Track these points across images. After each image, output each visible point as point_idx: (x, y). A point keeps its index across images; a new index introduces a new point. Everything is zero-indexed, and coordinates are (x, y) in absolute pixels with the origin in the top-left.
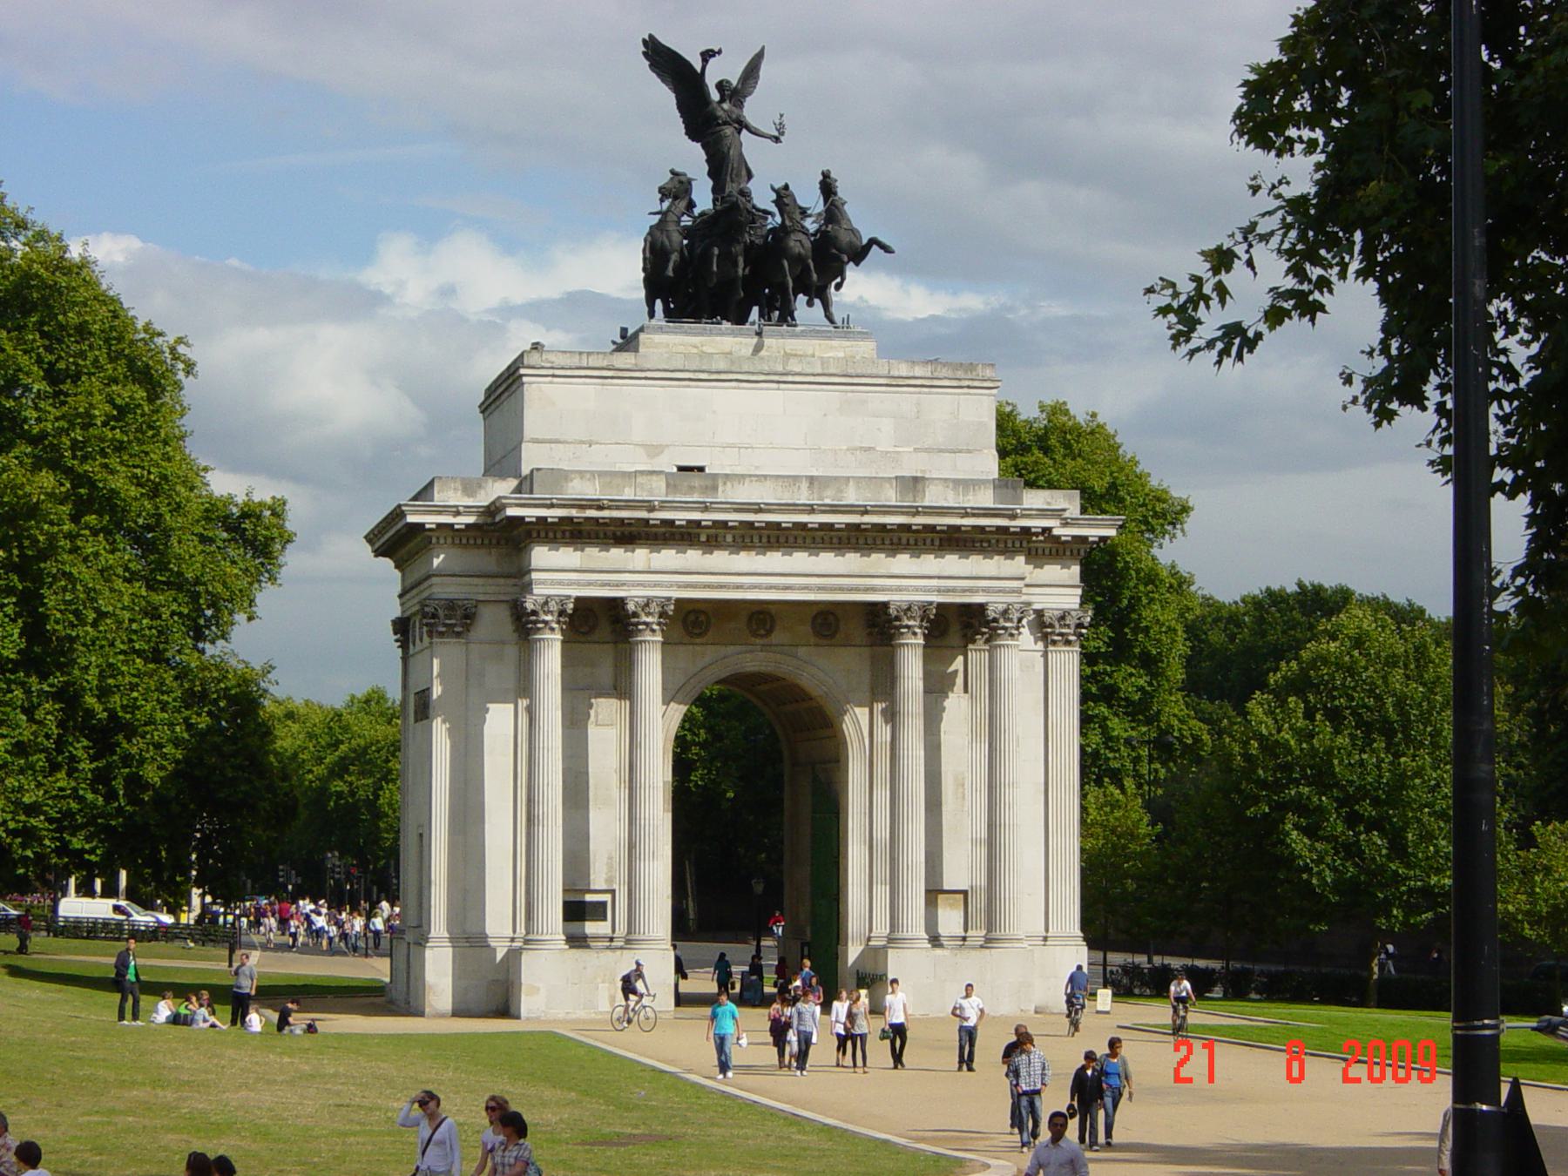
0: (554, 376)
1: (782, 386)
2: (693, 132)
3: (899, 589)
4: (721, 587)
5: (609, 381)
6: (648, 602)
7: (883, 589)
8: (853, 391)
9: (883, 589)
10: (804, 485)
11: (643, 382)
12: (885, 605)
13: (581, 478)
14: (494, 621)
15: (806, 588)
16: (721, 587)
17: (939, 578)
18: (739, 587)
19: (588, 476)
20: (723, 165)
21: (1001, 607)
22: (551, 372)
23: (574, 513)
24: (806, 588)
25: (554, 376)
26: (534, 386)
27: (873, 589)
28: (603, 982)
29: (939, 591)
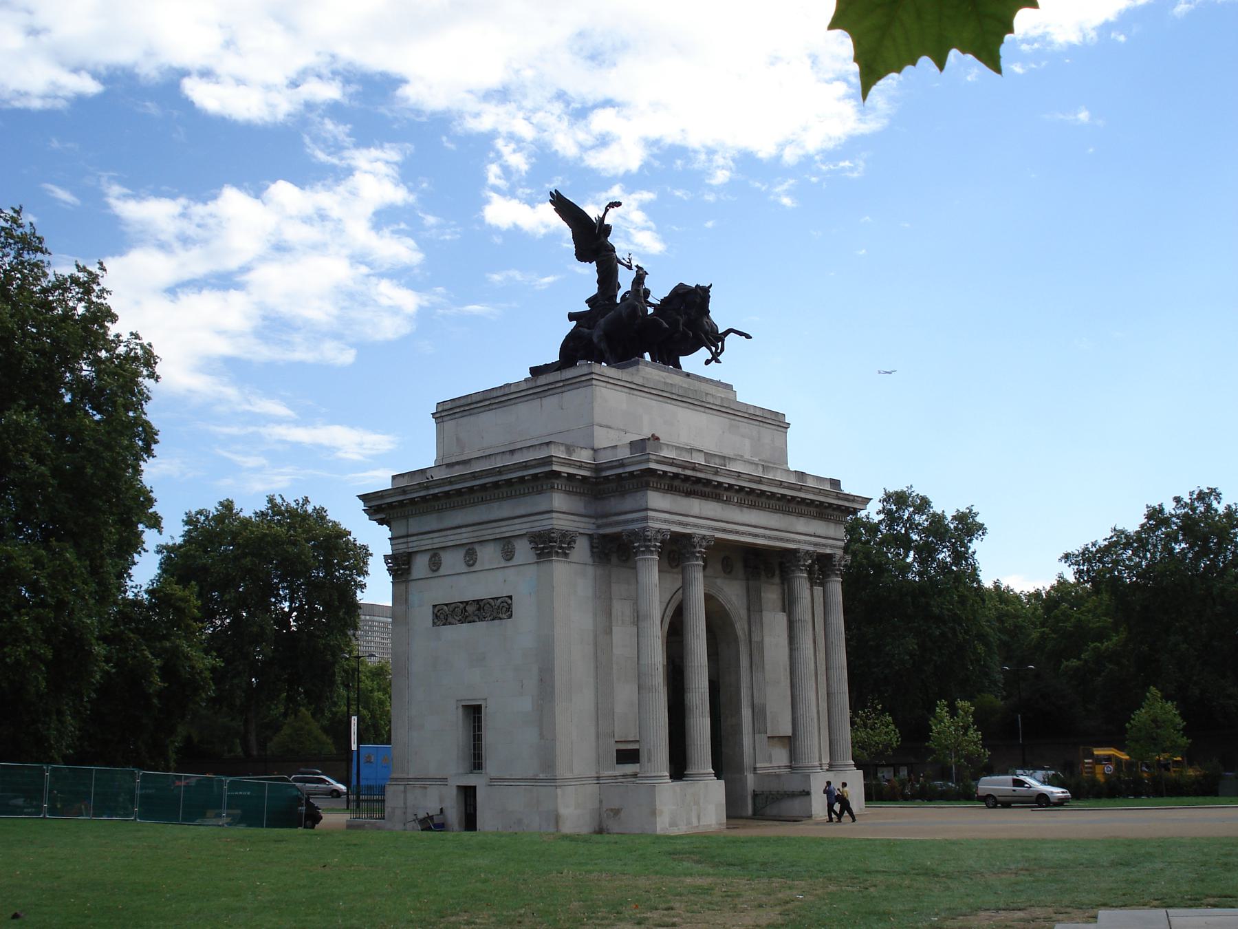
0: (608, 382)
1: (707, 410)
2: (582, 255)
3: (799, 542)
4: (730, 532)
5: (632, 392)
6: (704, 537)
7: (793, 541)
8: (734, 420)
9: (793, 541)
10: (760, 468)
11: (647, 395)
12: (796, 551)
13: (668, 449)
14: (581, 549)
15: (764, 537)
16: (730, 532)
17: (815, 536)
18: (737, 533)
19: (670, 448)
20: (607, 278)
21: (838, 557)
22: (606, 379)
23: (680, 471)
24: (764, 537)
25: (608, 382)
26: (597, 387)
27: (788, 540)
28: (694, 805)
29: (816, 544)
